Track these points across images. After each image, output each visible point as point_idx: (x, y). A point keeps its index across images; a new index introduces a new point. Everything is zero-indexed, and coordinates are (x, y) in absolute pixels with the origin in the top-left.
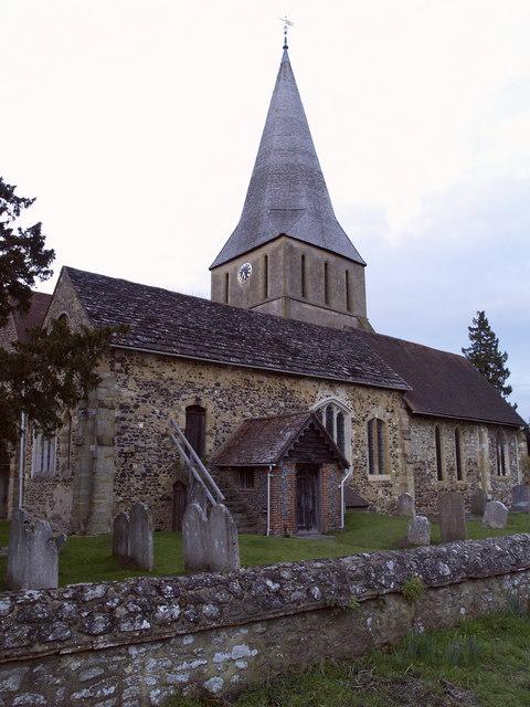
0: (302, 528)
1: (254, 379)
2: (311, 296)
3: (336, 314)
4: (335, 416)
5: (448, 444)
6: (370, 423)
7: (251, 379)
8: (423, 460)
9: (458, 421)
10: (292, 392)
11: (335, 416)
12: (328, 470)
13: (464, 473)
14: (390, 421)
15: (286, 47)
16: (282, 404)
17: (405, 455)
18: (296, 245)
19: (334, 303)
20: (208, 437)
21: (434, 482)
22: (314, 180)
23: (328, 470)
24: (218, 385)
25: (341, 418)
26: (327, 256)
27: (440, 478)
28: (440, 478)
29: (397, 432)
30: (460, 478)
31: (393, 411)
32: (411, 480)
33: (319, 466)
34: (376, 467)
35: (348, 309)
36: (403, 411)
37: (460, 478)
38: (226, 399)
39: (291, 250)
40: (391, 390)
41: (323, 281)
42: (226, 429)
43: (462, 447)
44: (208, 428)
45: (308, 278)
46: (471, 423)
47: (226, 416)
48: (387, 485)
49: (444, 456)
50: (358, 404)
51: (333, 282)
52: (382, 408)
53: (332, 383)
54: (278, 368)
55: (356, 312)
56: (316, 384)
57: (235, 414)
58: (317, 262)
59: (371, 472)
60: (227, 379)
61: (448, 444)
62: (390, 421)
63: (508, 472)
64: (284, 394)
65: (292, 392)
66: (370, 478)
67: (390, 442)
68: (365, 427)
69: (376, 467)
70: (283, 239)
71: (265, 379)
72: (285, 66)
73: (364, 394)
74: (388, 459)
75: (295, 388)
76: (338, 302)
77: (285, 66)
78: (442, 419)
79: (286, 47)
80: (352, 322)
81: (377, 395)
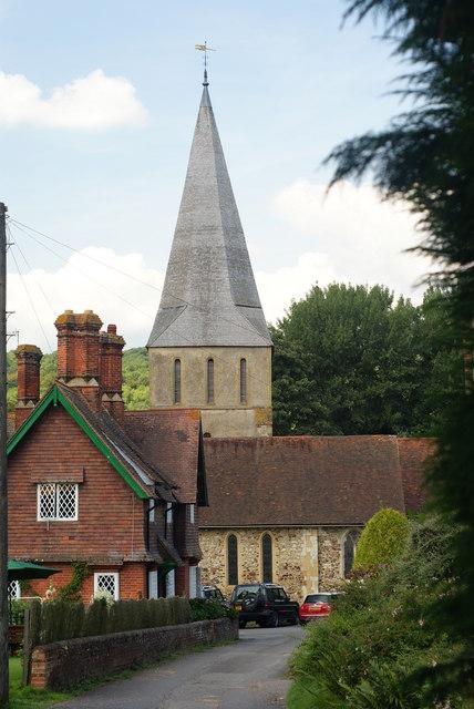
18: (164, 352)
19: (219, 400)
26: (208, 353)
39: (159, 359)
41: (204, 381)
43: (275, 551)
46: (294, 528)
51: (218, 379)
58: (196, 363)
72: (207, 106)
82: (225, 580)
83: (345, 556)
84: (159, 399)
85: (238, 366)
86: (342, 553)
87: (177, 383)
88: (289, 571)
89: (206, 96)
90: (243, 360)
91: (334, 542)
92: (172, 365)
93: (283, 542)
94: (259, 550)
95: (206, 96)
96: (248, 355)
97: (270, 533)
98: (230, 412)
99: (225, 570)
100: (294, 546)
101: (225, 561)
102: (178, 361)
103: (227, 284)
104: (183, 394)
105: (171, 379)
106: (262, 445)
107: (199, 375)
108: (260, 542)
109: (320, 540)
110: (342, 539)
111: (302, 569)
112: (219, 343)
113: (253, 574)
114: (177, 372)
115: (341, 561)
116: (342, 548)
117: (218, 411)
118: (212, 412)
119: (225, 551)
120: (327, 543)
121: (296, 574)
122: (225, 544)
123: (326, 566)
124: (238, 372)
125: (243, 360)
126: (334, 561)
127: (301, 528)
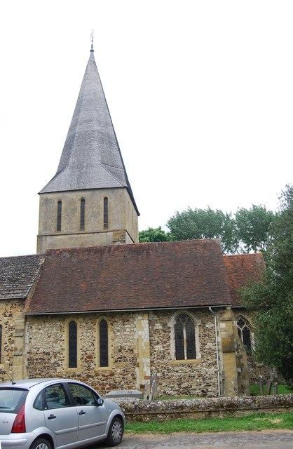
5: (88, 337)
8: (49, 351)
9: (105, 314)
13: (111, 360)
14: (6, 323)
15: (92, 51)
18: (50, 196)
19: (88, 228)
31: (11, 315)
40: (9, 300)
43: (110, 335)
46: (127, 314)
51: (88, 213)
58: (72, 202)
61: (88, 337)
63: (199, 355)
72: (92, 63)
76: (94, 223)
77: (92, 63)
78: (77, 316)
79: (92, 51)
82: (66, 362)
83: (176, 338)
85: (102, 202)
86: (172, 335)
87: (59, 217)
88: (123, 354)
89: (92, 56)
90: (106, 199)
91: (164, 325)
92: (56, 204)
93: (118, 326)
94: (96, 334)
95: (92, 56)
96: (109, 194)
97: (105, 318)
98: (95, 234)
99: (66, 354)
100: (128, 330)
101: (66, 346)
102: (60, 202)
103: (97, 151)
104: (62, 224)
105: (55, 214)
106: (110, 250)
108: (97, 327)
109: (150, 323)
110: (172, 323)
111: (135, 351)
113: (90, 357)
114: (59, 210)
115: (172, 343)
116: (173, 331)
117: (86, 235)
118: (83, 235)
119: (65, 336)
120: (158, 326)
121: (129, 356)
122: (66, 330)
123: (158, 348)
124: (102, 207)
125: (106, 199)
126: (165, 342)
127: (134, 313)
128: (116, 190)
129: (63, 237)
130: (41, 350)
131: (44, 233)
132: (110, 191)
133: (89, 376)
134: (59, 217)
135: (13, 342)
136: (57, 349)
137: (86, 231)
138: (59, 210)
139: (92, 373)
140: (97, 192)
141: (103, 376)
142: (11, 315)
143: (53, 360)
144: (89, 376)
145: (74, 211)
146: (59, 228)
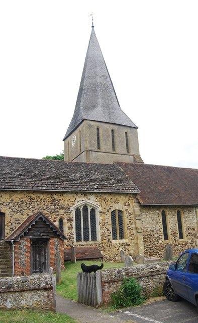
0: (36, 272)
1: (34, 196)
2: (103, 147)
3: (120, 155)
4: (89, 211)
5: (172, 220)
6: (113, 212)
7: (32, 196)
8: (153, 229)
9: (179, 207)
10: (59, 201)
11: (89, 211)
12: (54, 242)
13: (185, 235)
14: (127, 210)
15: (93, 27)
16: (53, 207)
17: (137, 228)
18: (92, 123)
19: (118, 150)
20: (6, 227)
21: (162, 241)
22: (108, 89)
23: (54, 242)
24: (12, 200)
25: (93, 211)
26: (112, 127)
27: (166, 238)
28: (166, 238)
29: (132, 216)
30: (181, 237)
31: (129, 205)
32: (141, 242)
33: (48, 239)
34: (118, 236)
35: (128, 151)
36: (136, 204)
37: (181, 237)
38: (17, 208)
39: (90, 126)
40: (127, 194)
41: (111, 139)
42: (17, 222)
43: (183, 220)
44: (6, 222)
45: (101, 139)
47: (17, 216)
48: (125, 245)
49: (169, 226)
50: (104, 203)
51: (117, 140)
52: (119, 204)
53: (85, 194)
54: (48, 189)
55: (132, 152)
56: (75, 196)
57: (22, 214)
58: (106, 131)
59: (115, 238)
60: (17, 198)
61: (172, 220)
62: (127, 210)
64: (53, 202)
65: (59, 201)
66: (114, 242)
67: (128, 222)
68: (109, 215)
69: (118, 236)
70: (85, 121)
71: (42, 195)
72: (93, 36)
73: (108, 198)
74: (126, 231)
75: (61, 198)
76: (121, 148)
77: (93, 36)
78: (166, 207)
79: (93, 27)
80: (128, 159)
81: (117, 197)
84: (91, 145)
87: (98, 139)
89: (93, 30)
90: (126, 133)
94: (176, 219)
95: (93, 30)
100: (191, 217)
107: (108, 137)
112: (117, 123)
114: (98, 134)
117: (118, 155)
118: (115, 155)
128: (132, 129)
129: (103, 153)
130: (149, 229)
131: (90, 149)
132: (129, 128)
133: (176, 245)
134: (98, 139)
135: (132, 224)
136: (158, 228)
137: (117, 152)
138: (98, 134)
139: (177, 244)
140: (122, 127)
141: (182, 244)
142: (129, 205)
143: (156, 236)
144: (176, 245)
145: (108, 137)
146: (99, 147)
